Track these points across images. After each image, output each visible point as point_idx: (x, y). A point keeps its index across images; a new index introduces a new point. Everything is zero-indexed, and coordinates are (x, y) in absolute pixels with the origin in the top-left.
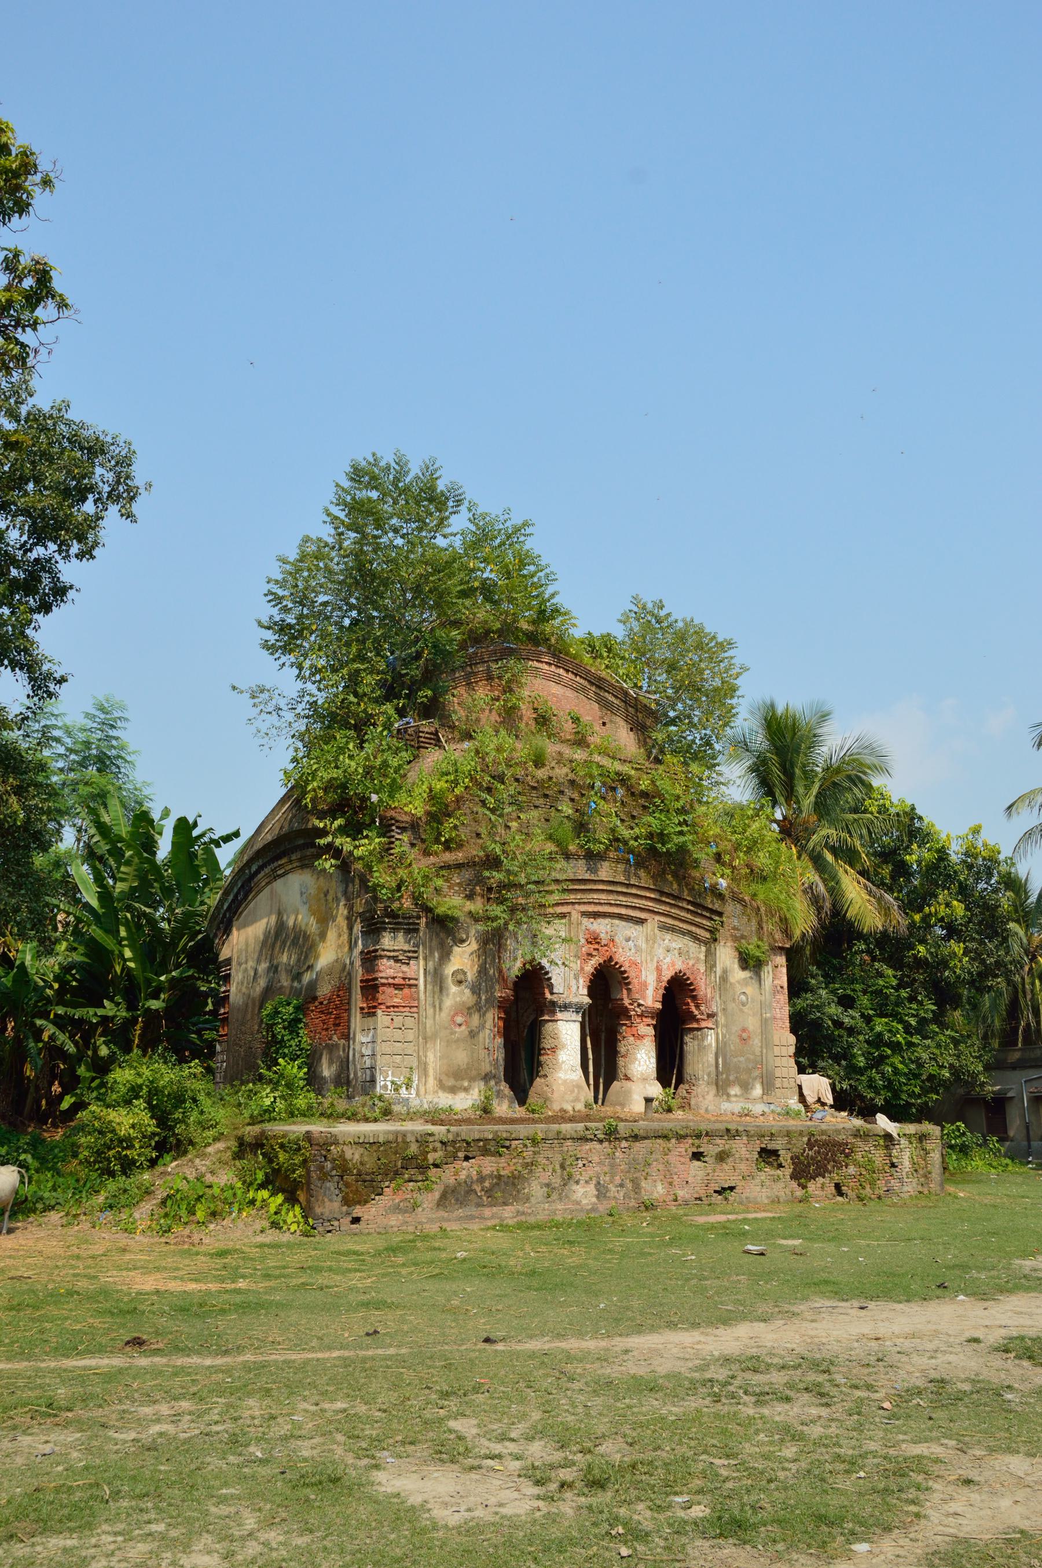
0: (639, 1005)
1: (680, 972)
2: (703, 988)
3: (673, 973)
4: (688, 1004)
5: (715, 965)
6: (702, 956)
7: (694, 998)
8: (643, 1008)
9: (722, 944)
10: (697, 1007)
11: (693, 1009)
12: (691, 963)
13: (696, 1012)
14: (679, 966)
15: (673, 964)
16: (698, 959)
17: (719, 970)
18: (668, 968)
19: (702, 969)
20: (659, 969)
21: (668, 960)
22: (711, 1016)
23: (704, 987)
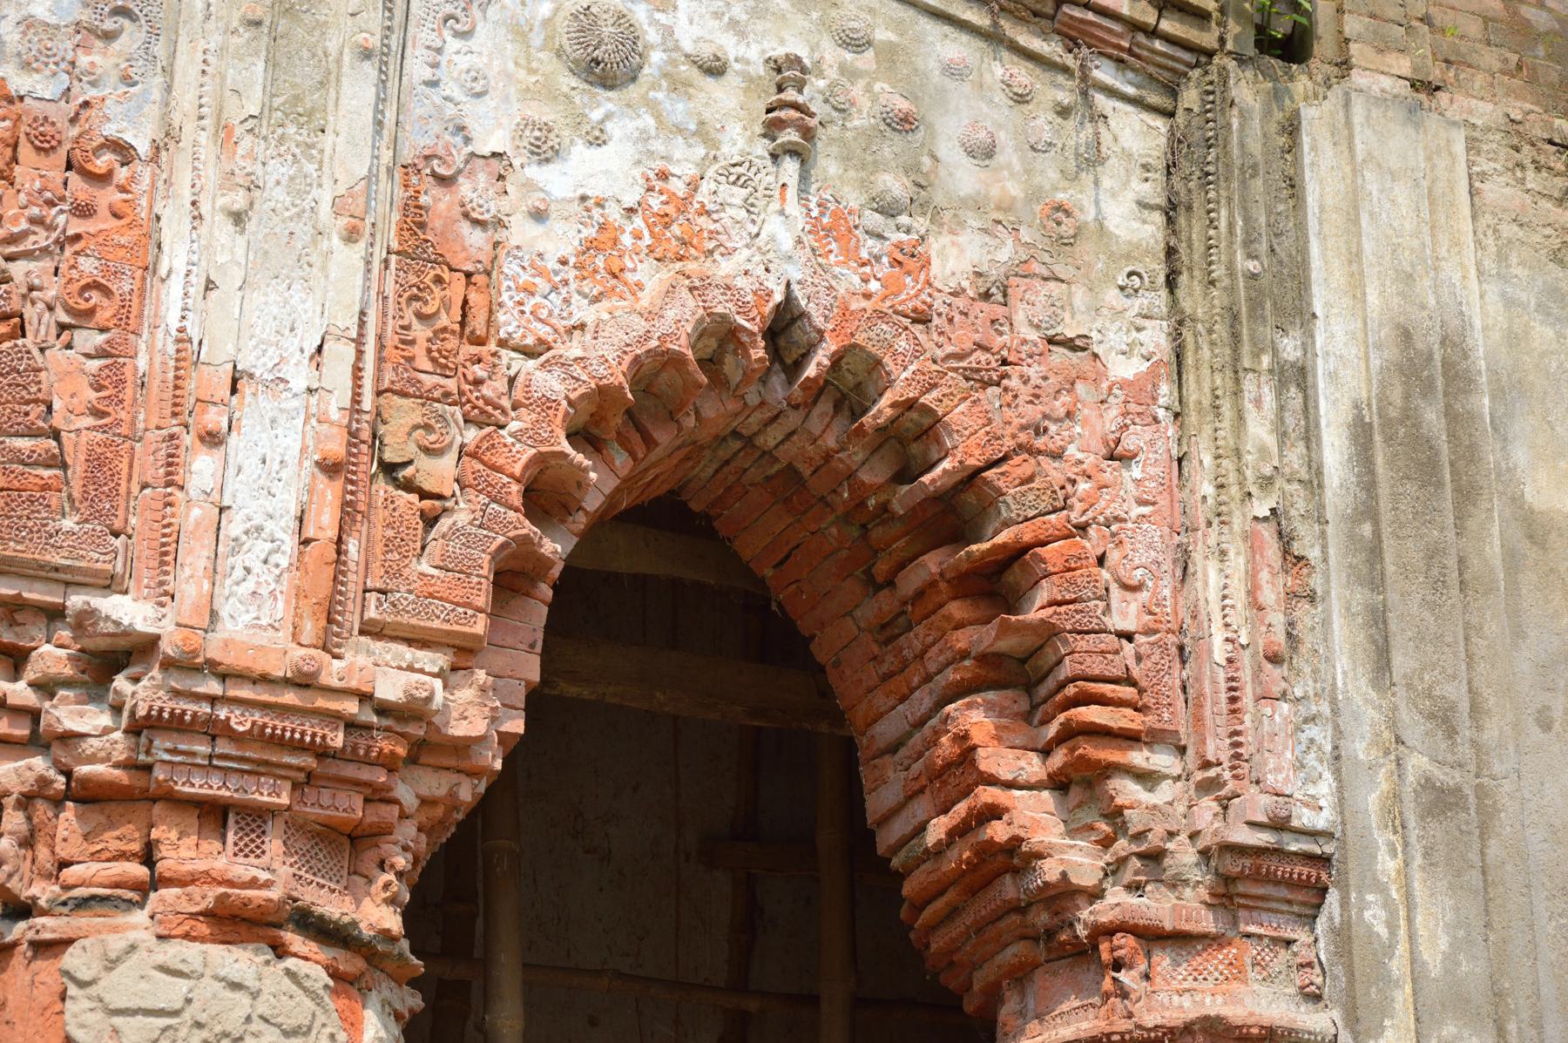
0: (110, 658)
1: (785, 325)
2: (1143, 551)
3: (678, 325)
4: (963, 767)
5: (1283, 296)
6: (1123, 210)
7: (1023, 675)
8: (141, 691)
9: (1379, 77)
10: (1078, 784)
11: (1035, 817)
12: (956, 258)
13: (1070, 857)
14: (767, 250)
15: (677, 227)
16: (1063, 232)
17: (1344, 352)
18: (600, 259)
19: (1129, 343)
20: (429, 258)
21: (605, 166)
22: (1275, 879)
23: (1170, 531)
